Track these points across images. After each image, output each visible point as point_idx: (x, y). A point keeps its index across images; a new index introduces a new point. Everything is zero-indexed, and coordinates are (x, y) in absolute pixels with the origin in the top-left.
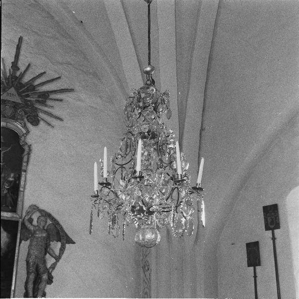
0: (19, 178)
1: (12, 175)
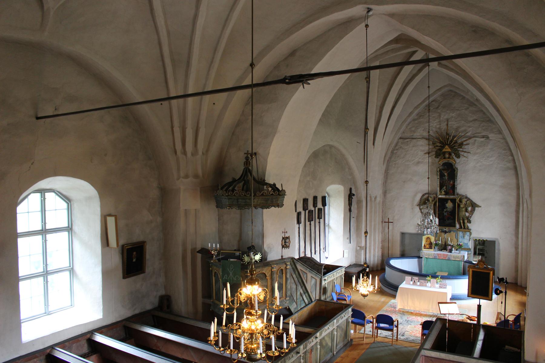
0: (454, 182)
1: (452, 181)
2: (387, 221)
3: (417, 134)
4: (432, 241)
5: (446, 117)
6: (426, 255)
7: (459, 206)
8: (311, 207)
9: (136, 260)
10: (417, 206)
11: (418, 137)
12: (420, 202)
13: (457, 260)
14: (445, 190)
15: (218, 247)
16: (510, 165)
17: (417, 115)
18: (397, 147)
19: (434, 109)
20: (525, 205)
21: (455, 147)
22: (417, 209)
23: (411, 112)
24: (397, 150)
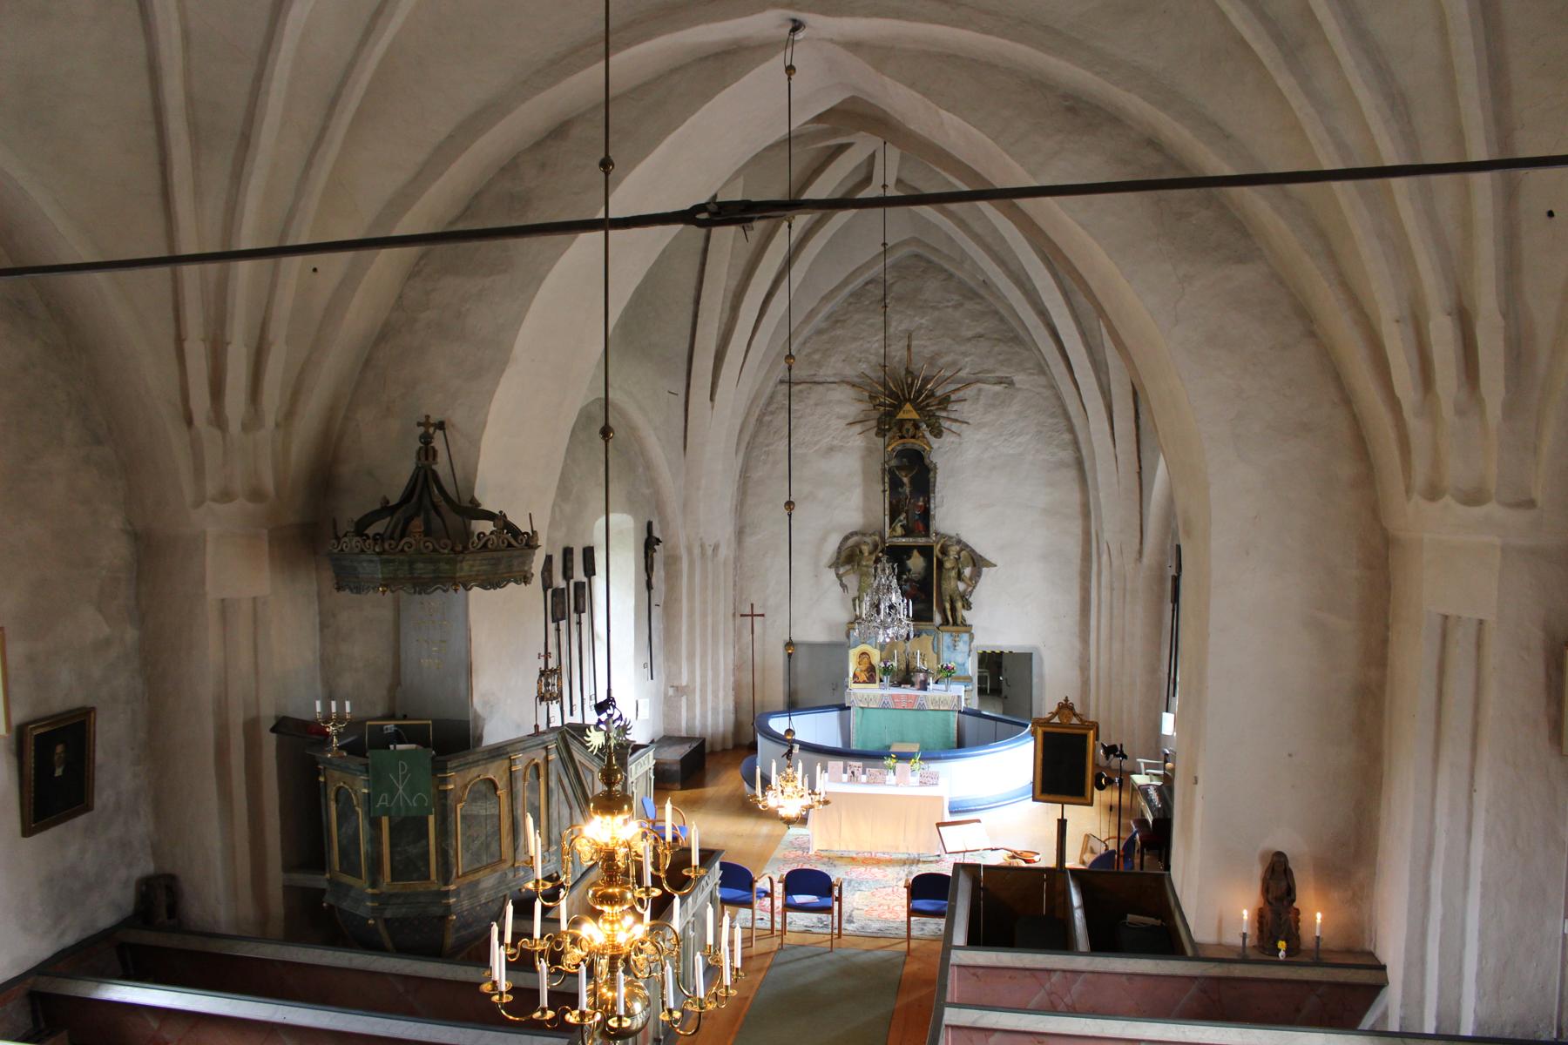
0: (928, 501)
1: (921, 499)
2: (748, 611)
3: (826, 372)
4: (873, 663)
5: (903, 327)
6: (861, 701)
7: (940, 564)
8: (559, 582)
9: (64, 771)
10: (830, 567)
11: (829, 380)
12: (838, 558)
13: (941, 708)
14: (905, 522)
15: (348, 709)
16: (1067, 455)
17: (828, 318)
18: (772, 408)
19: (871, 303)
20: (1105, 558)
21: (928, 409)
22: (831, 574)
23: (812, 310)
24: (772, 413)
